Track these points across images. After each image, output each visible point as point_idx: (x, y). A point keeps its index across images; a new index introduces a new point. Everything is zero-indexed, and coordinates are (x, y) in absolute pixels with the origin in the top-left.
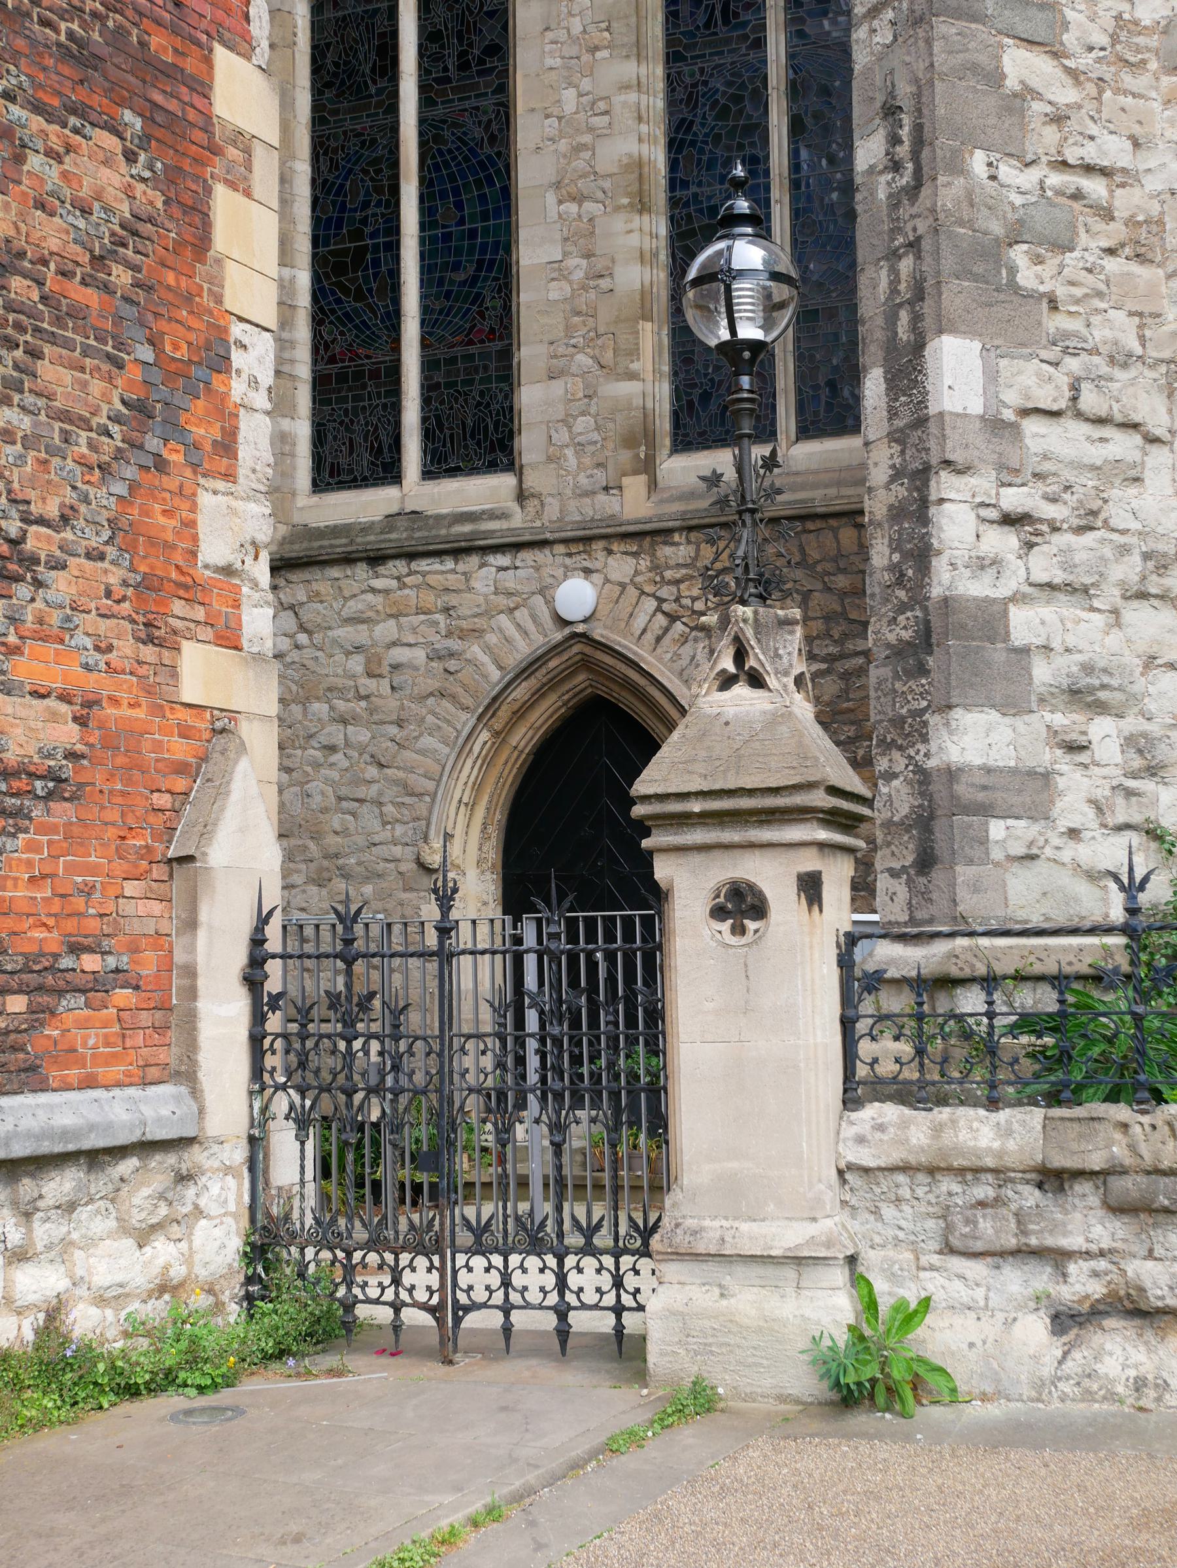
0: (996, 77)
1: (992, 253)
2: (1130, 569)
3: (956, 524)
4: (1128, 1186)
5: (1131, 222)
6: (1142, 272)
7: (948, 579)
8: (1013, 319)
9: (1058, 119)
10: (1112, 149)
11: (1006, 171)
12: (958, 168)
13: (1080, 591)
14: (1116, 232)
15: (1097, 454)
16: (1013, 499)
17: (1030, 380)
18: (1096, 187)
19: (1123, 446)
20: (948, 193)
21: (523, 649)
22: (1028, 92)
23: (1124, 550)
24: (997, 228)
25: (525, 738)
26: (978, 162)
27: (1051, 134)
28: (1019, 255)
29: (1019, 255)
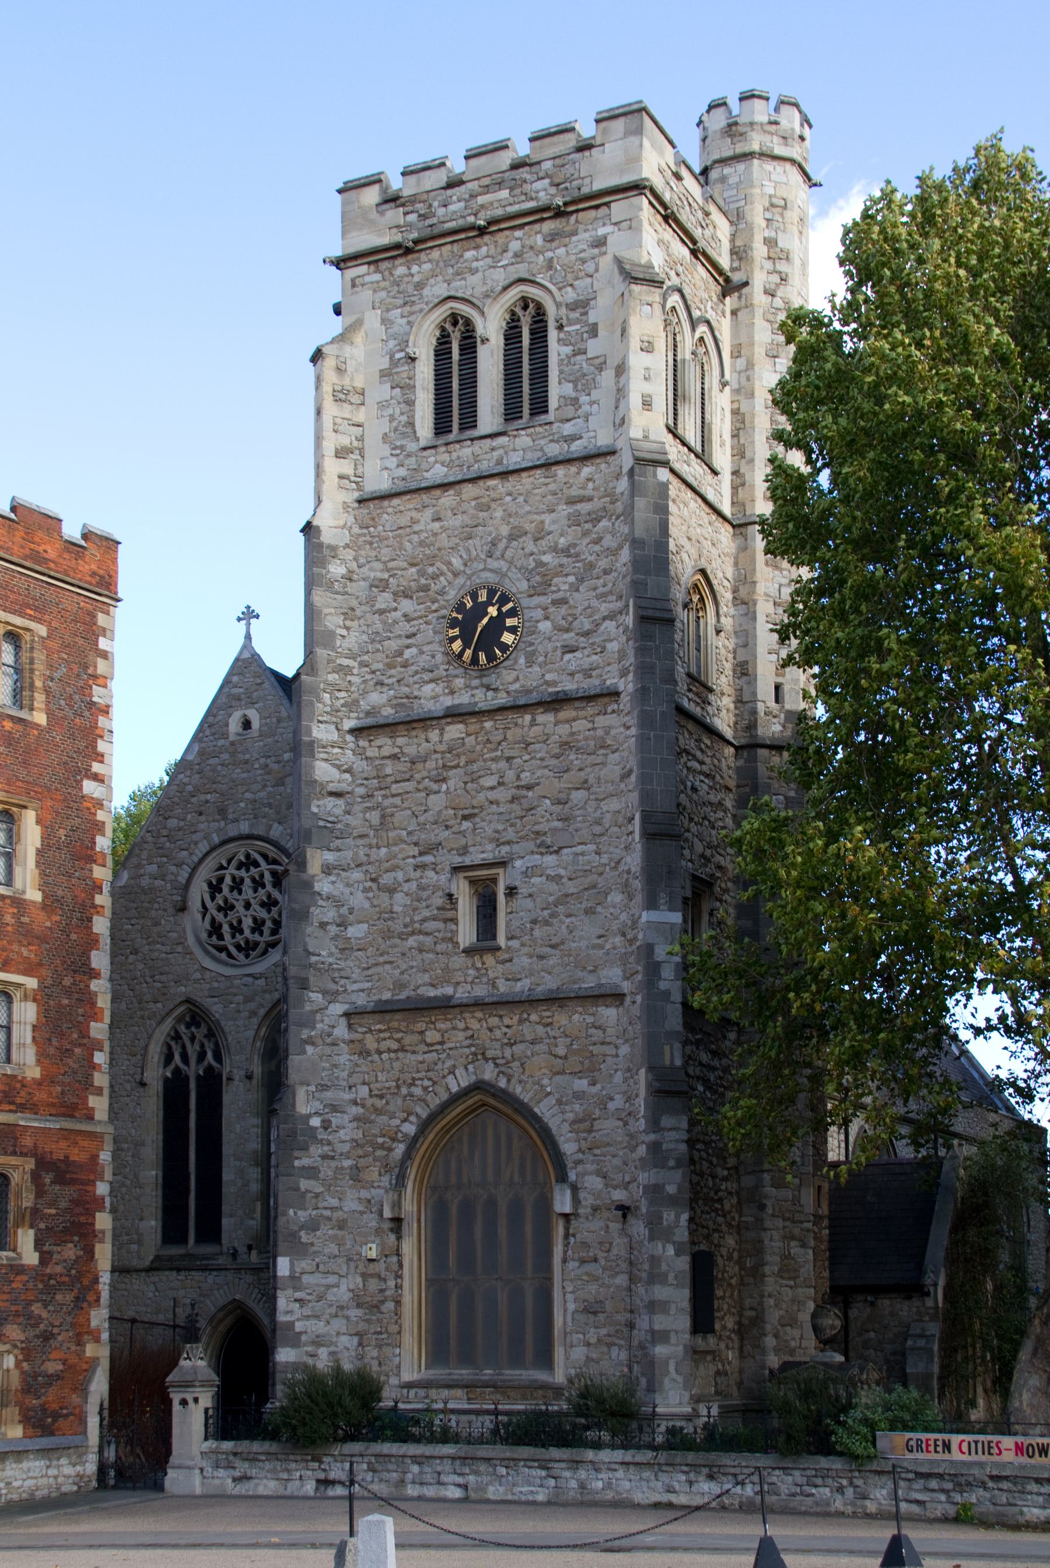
0: (298, 1189)
1: (294, 1235)
2: (333, 1310)
3: (282, 1303)
4: (245, 1456)
5: (338, 1221)
6: (340, 1233)
7: (281, 1318)
8: (299, 1250)
9: (317, 1196)
10: (334, 1202)
11: (300, 1213)
12: (285, 1214)
13: (317, 1317)
14: (334, 1222)
15: (324, 1282)
16: (298, 1295)
17: (304, 1264)
18: (328, 1213)
19: (332, 1279)
20: (281, 1221)
21: (222, 1302)
22: (307, 1191)
23: (331, 1306)
24: (296, 1228)
25: (222, 1328)
26: (291, 1212)
27: (314, 1201)
28: (302, 1233)
29: (302, 1233)
